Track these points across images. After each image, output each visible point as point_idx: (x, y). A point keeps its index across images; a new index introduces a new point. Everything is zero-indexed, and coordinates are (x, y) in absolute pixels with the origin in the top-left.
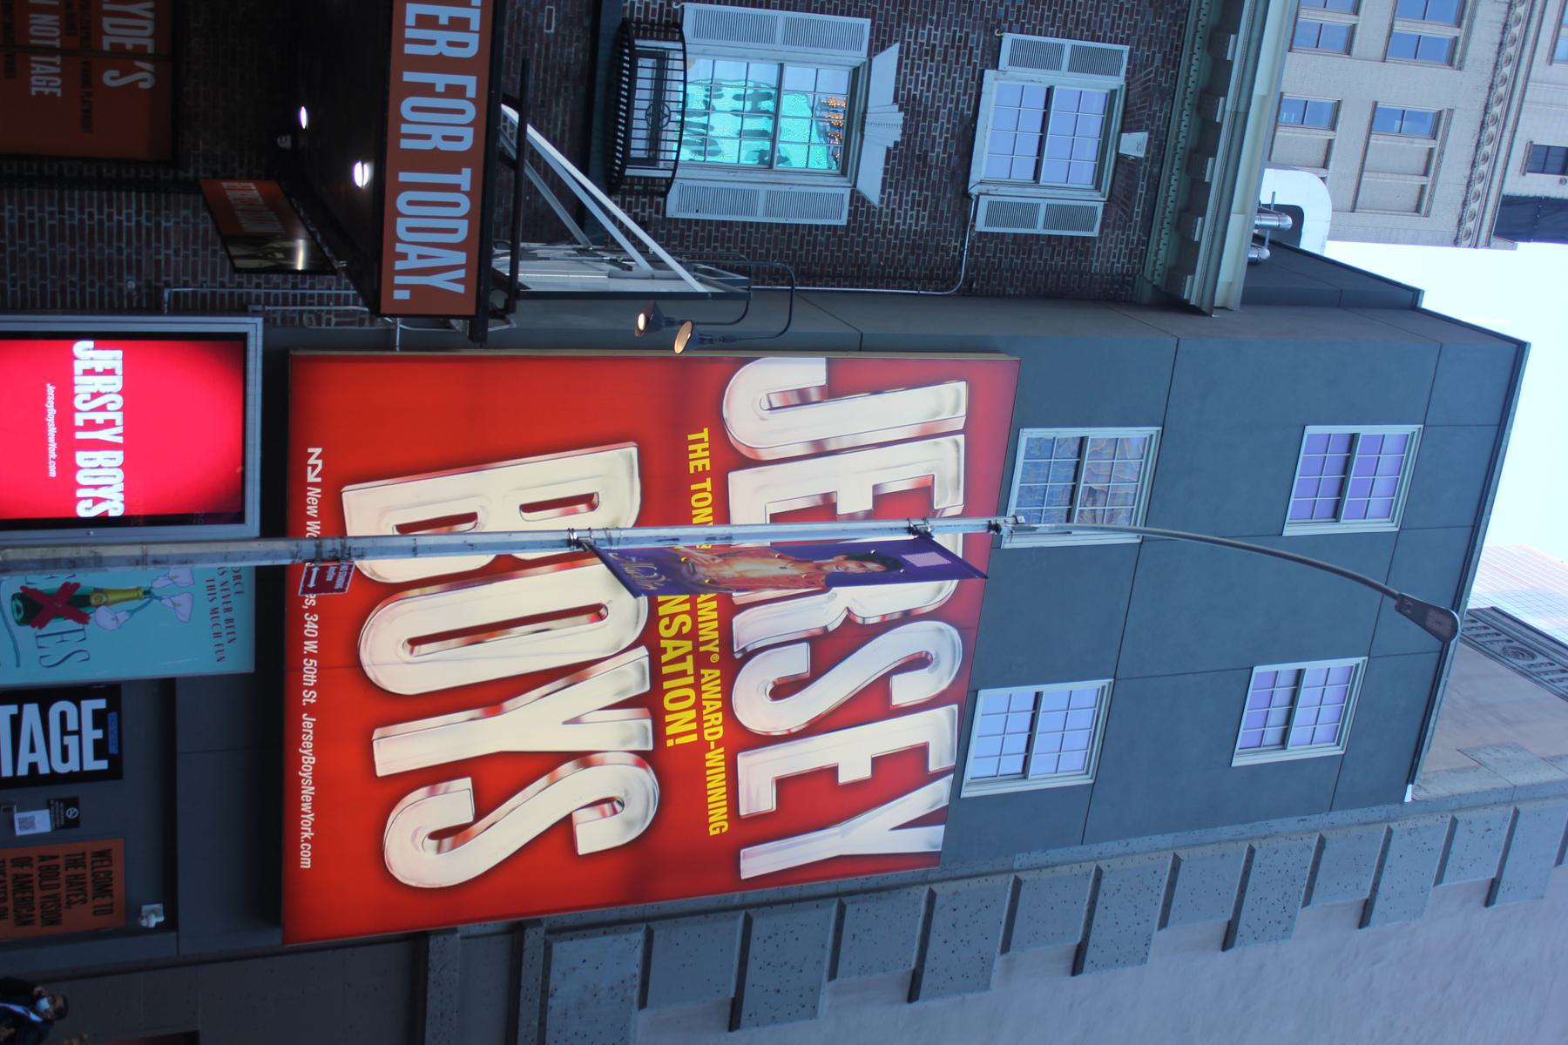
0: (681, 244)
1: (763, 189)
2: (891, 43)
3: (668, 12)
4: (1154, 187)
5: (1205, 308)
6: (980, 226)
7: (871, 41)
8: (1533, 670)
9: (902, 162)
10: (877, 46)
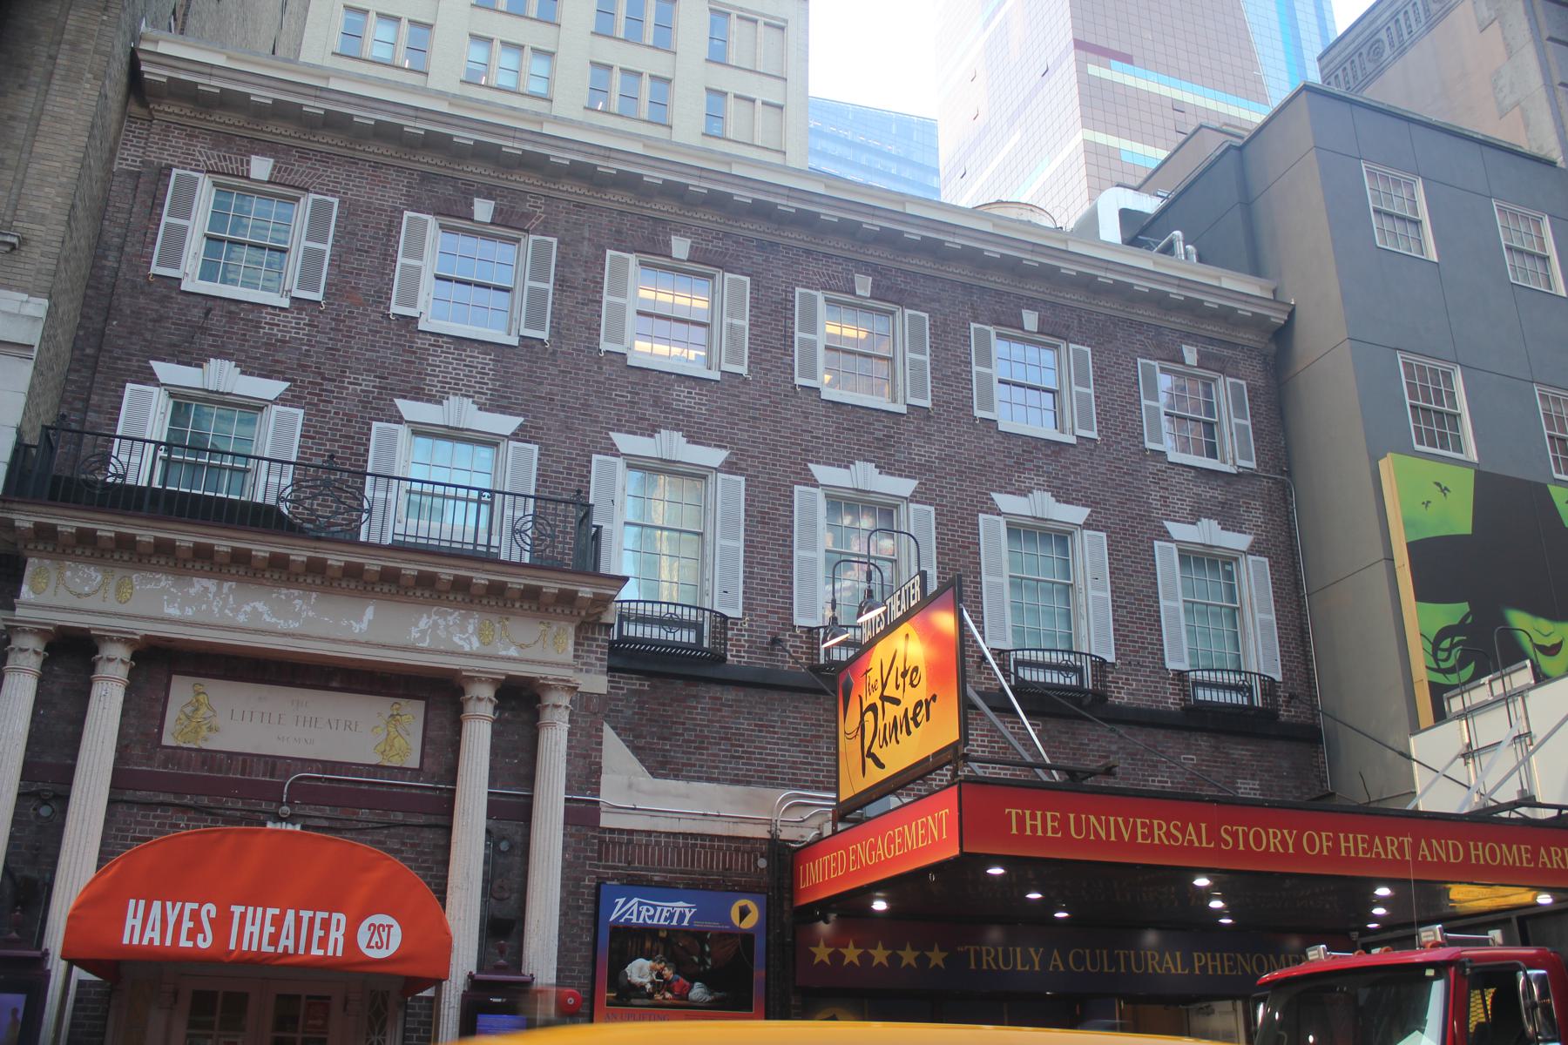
1: (1258, 616)
4: (1211, 341)
6: (1253, 465)
8: (1397, 44)
9: (1230, 522)
10: (1166, 536)
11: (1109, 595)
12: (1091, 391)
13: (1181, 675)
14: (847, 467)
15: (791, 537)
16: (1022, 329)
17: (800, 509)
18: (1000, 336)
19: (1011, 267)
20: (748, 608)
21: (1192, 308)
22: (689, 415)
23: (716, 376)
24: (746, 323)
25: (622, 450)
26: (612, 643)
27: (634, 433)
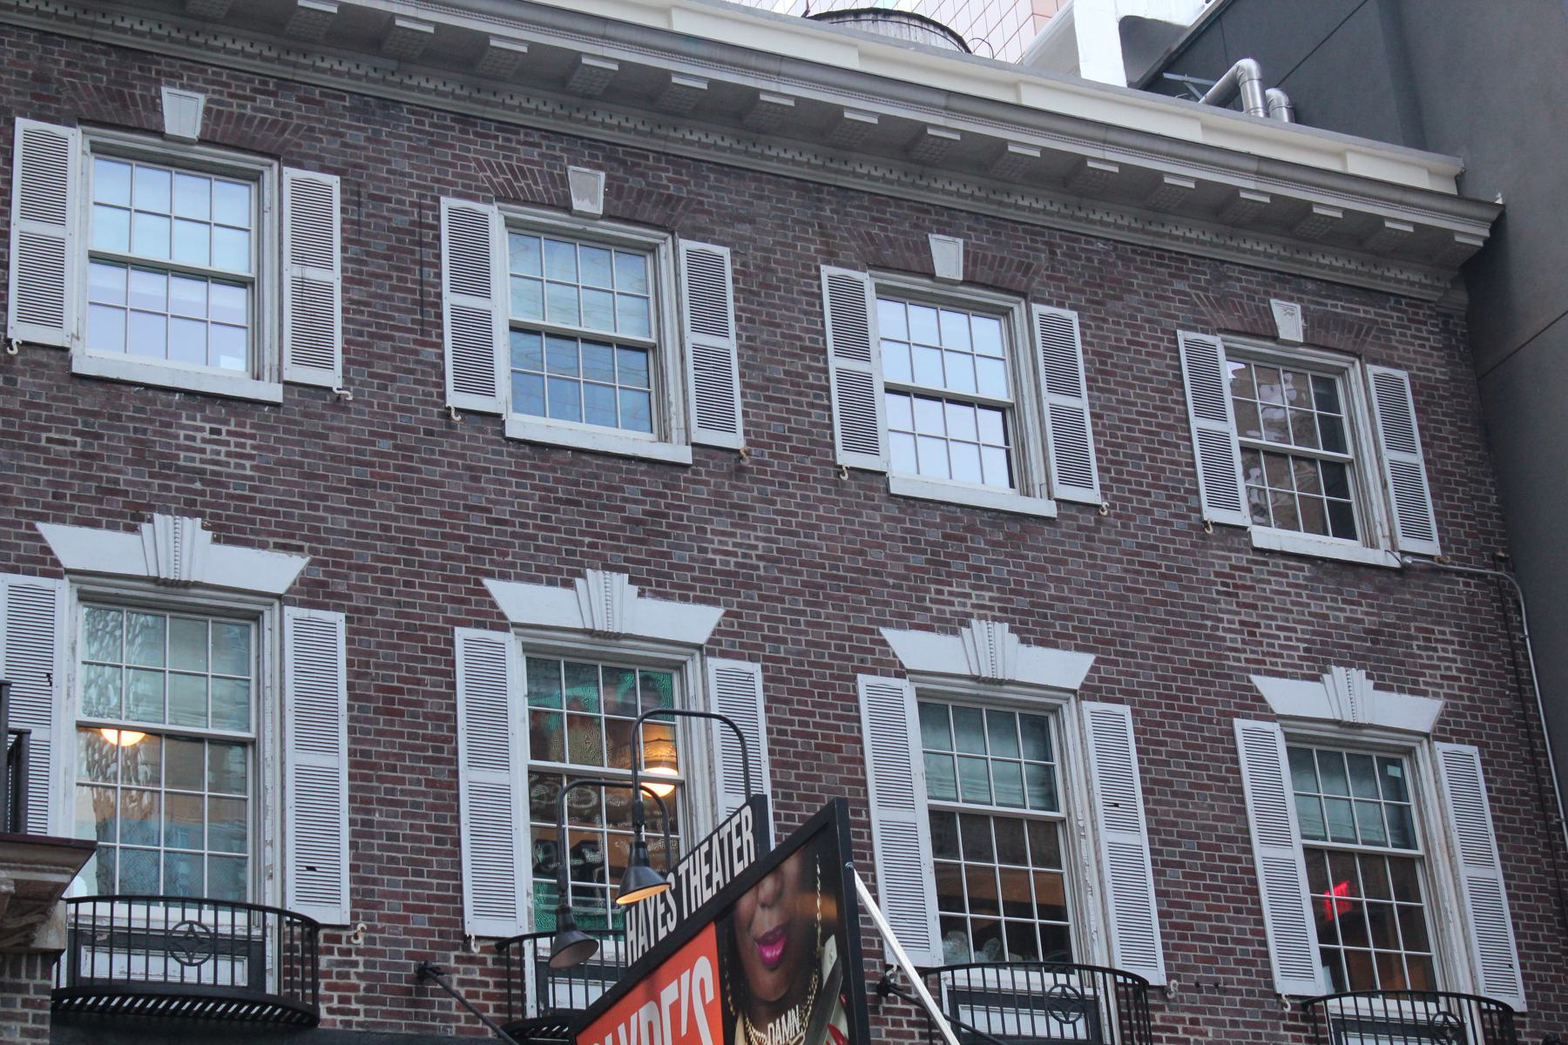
0: (1551, 988)
1: (1465, 872)
2: (1252, 688)
3: (1293, 1017)
5: (1494, 215)
6: (1432, 548)
7: (1257, 718)
10: (1257, 706)
11: (1142, 839)
12: (1082, 403)
13: (1308, 1005)
14: (568, 584)
15: (452, 740)
16: (931, 275)
17: (469, 678)
18: (884, 292)
19: (907, 147)
20: (361, 902)
21: (1289, 222)
22: (216, 481)
23: (274, 393)
24: (334, 277)
25: (68, 561)
26: (58, 994)
27: (94, 524)
